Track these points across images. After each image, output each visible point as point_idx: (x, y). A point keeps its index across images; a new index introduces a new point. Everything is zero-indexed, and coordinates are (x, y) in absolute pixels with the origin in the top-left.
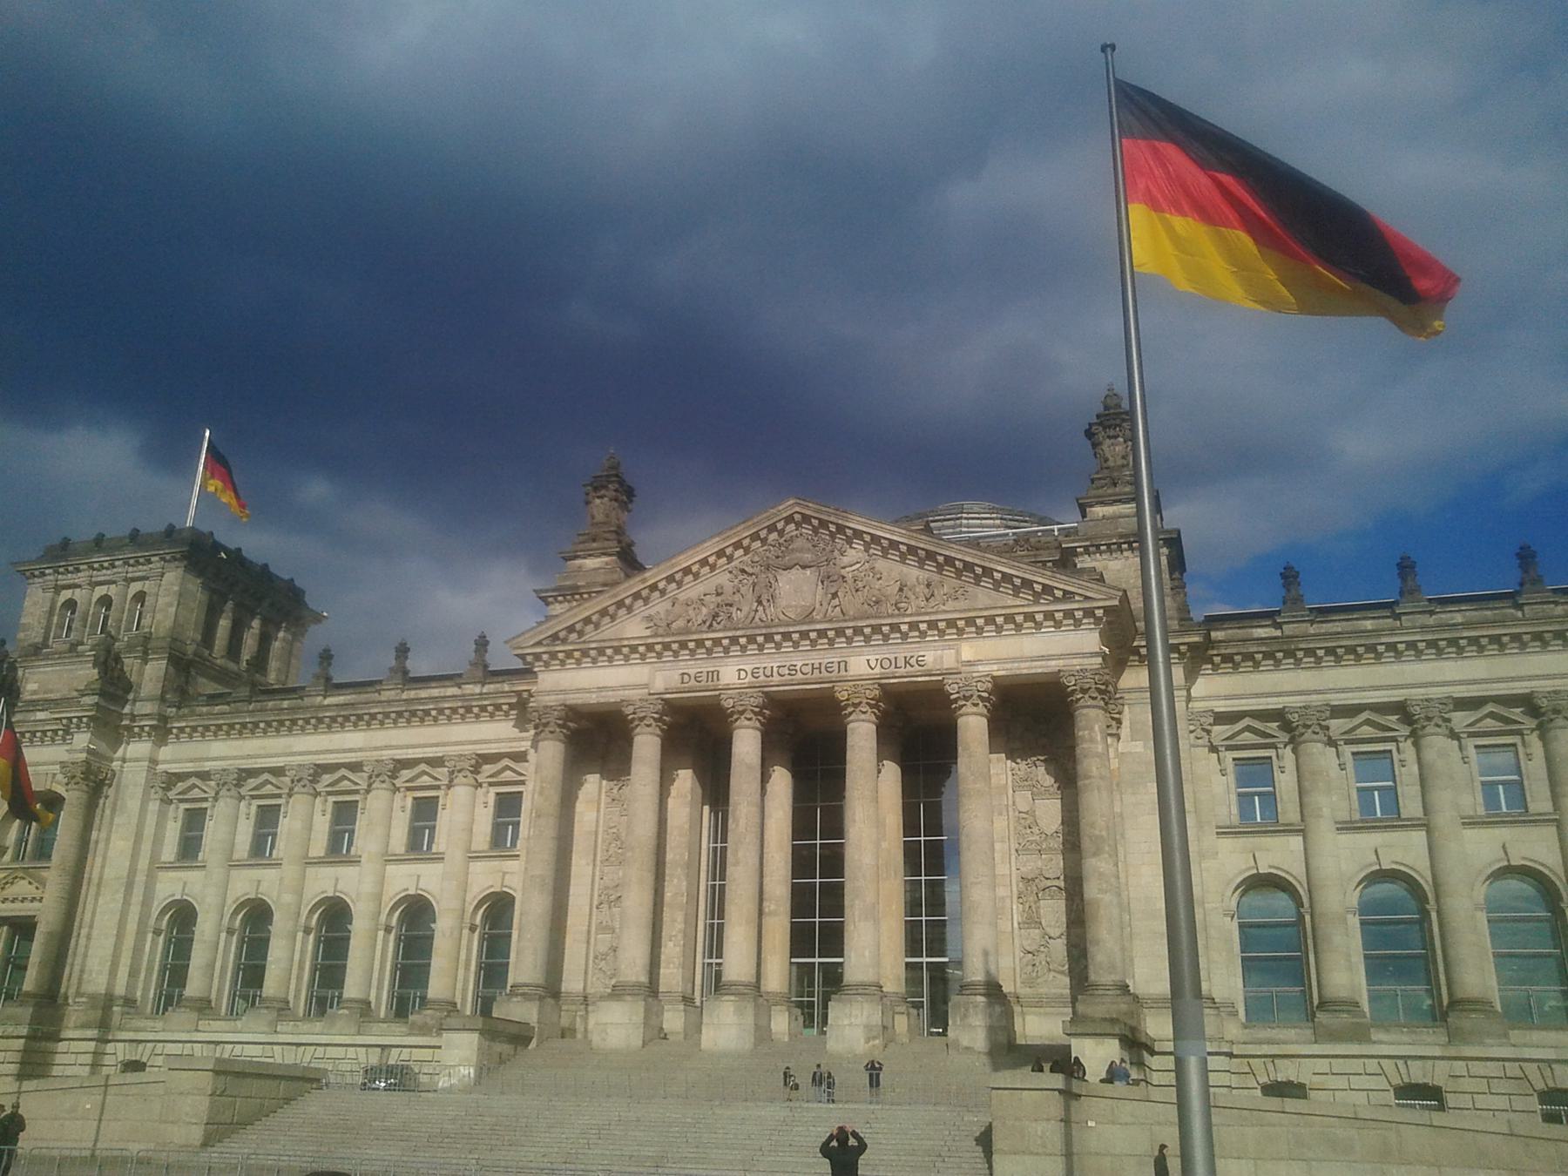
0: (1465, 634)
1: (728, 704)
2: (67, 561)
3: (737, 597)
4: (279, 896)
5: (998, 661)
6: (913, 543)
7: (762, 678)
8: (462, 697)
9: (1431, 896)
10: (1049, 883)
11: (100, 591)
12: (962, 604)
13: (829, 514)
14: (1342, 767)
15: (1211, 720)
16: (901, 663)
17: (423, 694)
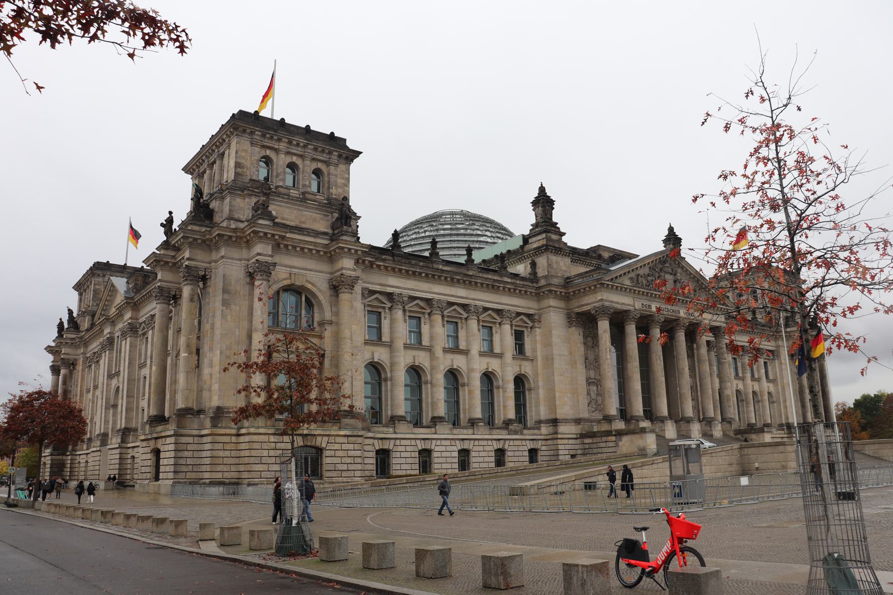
17: (485, 276)
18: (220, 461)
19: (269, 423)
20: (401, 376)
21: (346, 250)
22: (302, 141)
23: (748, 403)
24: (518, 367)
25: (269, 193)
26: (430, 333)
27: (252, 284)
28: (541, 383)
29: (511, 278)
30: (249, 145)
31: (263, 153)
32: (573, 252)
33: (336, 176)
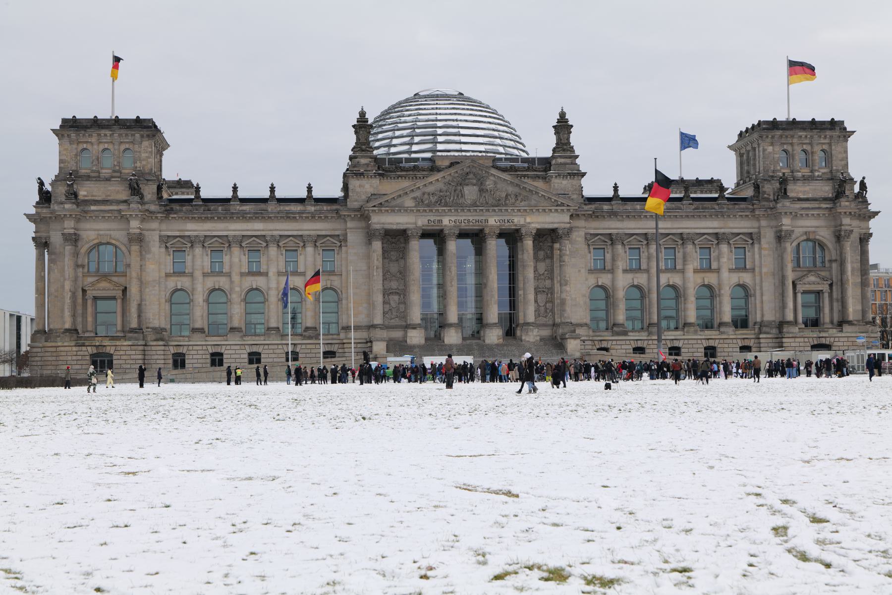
0: (667, 214)
1: (446, 232)
2: (85, 131)
3: (448, 193)
4: (231, 289)
5: (538, 223)
6: (513, 181)
7: (458, 223)
8: (312, 213)
9: (647, 293)
10: (540, 290)
11: (102, 147)
12: (526, 203)
13: (483, 167)
14: (626, 252)
15: (589, 236)
16: (506, 221)
17: (287, 208)
18: (49, 363)
19: (72, 339)
20: (199, 298)
21: (128, 216)
22: (108, 133)
23: (685, 300)
24: (325, 282)
25: (72, 184)
26: (231, 261)
27: (64, 248)
28: (344, 295)
29: (315, 206)
30: (69, 145)
31: (81, 146)
32: (378, 173)
33: (140, 152)
